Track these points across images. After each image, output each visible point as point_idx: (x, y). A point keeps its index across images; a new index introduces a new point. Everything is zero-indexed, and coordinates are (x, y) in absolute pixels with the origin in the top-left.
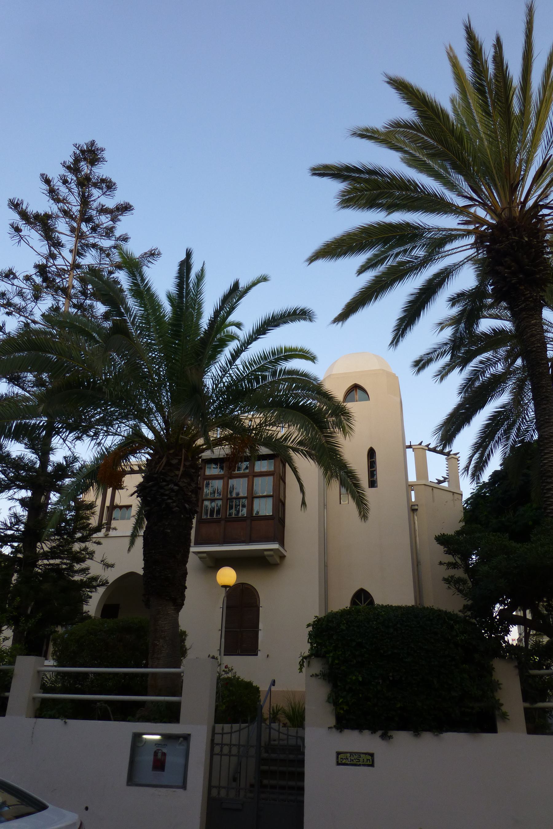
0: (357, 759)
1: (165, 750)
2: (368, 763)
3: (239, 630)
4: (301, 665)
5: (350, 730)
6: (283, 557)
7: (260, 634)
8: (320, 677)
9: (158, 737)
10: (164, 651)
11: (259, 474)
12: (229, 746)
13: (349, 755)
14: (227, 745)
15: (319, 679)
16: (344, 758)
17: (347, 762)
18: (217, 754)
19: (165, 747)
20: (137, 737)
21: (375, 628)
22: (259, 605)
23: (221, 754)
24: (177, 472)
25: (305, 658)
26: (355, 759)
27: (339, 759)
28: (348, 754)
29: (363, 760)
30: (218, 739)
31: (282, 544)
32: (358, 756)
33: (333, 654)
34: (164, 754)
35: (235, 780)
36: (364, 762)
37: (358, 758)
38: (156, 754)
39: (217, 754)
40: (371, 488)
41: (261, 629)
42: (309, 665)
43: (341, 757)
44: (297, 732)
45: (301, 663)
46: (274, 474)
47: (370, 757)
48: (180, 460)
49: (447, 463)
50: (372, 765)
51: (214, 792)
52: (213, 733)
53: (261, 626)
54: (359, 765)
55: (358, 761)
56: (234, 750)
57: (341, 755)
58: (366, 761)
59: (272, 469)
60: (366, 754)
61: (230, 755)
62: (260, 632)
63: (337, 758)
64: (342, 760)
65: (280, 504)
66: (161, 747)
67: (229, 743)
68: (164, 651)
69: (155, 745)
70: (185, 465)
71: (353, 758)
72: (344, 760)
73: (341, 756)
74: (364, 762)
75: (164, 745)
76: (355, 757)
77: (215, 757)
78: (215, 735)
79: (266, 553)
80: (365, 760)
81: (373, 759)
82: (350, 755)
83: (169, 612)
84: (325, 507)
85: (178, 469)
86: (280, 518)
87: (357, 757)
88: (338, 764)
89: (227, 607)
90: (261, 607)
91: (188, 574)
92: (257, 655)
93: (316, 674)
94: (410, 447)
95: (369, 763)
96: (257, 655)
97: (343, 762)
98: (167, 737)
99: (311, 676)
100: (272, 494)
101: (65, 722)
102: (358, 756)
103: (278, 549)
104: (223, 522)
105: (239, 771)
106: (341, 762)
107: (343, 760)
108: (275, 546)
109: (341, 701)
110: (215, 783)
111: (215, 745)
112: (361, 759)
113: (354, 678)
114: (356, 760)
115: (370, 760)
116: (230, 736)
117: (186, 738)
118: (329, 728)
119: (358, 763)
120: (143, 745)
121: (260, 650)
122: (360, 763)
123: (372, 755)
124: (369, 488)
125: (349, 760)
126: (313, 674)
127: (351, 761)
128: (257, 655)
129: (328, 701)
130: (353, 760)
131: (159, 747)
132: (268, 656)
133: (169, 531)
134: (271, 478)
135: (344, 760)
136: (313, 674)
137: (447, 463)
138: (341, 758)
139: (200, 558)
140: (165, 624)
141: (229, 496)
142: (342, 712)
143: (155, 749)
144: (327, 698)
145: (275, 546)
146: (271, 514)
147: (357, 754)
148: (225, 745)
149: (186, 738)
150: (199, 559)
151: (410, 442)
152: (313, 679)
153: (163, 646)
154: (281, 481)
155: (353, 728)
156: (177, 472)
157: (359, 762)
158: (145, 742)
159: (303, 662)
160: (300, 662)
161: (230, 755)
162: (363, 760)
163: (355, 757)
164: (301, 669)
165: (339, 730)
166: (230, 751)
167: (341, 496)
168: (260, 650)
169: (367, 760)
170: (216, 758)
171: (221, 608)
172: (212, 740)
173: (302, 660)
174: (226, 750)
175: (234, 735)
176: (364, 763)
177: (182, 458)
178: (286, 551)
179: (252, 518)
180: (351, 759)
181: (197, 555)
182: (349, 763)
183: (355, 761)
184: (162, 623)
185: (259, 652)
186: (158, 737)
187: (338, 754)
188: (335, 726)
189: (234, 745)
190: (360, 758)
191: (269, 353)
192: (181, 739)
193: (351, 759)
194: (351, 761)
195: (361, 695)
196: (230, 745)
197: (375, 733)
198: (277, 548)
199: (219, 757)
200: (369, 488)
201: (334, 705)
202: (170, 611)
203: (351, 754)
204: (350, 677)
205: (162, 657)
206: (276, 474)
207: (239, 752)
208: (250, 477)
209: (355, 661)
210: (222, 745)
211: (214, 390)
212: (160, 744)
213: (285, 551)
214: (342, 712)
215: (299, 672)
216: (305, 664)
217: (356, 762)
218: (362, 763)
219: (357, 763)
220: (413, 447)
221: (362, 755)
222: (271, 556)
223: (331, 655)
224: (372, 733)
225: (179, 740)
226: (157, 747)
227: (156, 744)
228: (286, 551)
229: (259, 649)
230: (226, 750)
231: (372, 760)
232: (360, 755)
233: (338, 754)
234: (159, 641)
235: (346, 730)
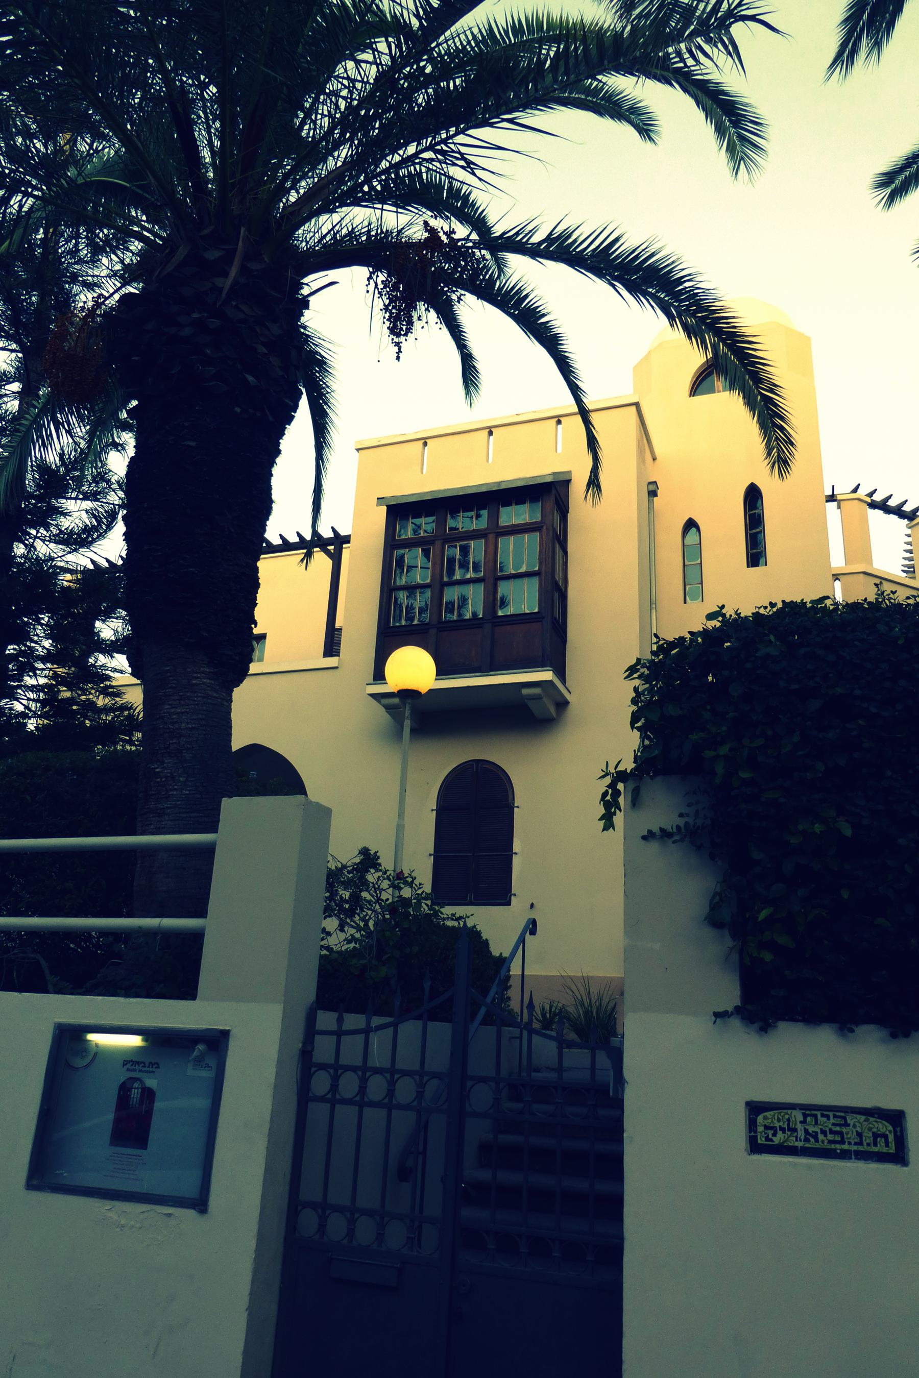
0: (832, 1132)
1: (151, 1082)
2: (881, 1147)
4: (610, 805)
5: (800, 1025)
6: (562, 705)
7: (516, 861)
8: (677, 838)
9: (135, 1041)
10: (176, 790)
11: (510, 529)
12: (360, 1073)
13: (798, 1115)
14: (354, 1069)
15: (674, 842)
16: (777, 1125)
17: (792, 1142)
18: (322, 1099)
19: (153, 1072)
21: (901, 642)
22: (514, 804)
23: (333, 1099)
24: (219, 281)
25: (621, 776)
26: (824, 1132)
27: (760, 1129)
28: (794, 1113)
29: (859, 1135)
30: (324, 1049)
31: (561, 673)
32: (839, 1121)
33: (731, 750)
34: (149, 1095)
35: (404, 1174)
36: (861, 1143)
37: (838, 1129)
38: (124, 1089)
39: (322, 1099)
40: (752, 567)
41: (517, 851)
42: (635, 802)
43: (767, 1122)
45: (608, 798)
46: (542, 527)
47: (884, 1127)
48: (232, 254)
49: (909, 531)
50: (899, 1157)
51: (309, 1221)
52: (311, 1032)
53: (517, 846)
54: (844, 1155)
55: (838, 1138)
56: (405, 1090)
57: (768, 1114)
58: (871, 1140)
59: (538, 517)
60: (868, 1112)
61: (389, 1104)
62: (515, 858)
63: (752, 1125)
64: (770, 1132)
65: (556, 595)
66: (140, 1071)
67: (358, 1062)
68: (176, 790)
69: (124, 1065)
70: (243, 269)
71: (817, 1129)
72: (780, 1133)
73: (765, 1118)
74: (861, 1143)
76: (828, 1124)
77: (312, 1106)
78: (317, 1037)
79: (525, 691)
80: (868, 1137)
81: (902, 1131)
82: (805, 1116)
83: (194, 682)
84: (654, 606)
85: (225, 274)
86: (555, 618)
87: (834, 1124)
88: (755, 1147)
89: (380, 680)
90: (518, 807)
91: (261, 586)
92: (510, 904)
93: (662, 830)
94: (831, 498)
95: (885, 1150)
97: (776, 1140)
99: (644, 838)
100: (537, 569)
102: (839, 1121)
103: (551, 682)
104: (433, 632)
105: (421, 1149)
106: (767, 1139)
107: (775, 1135)
108: (547, 675)
109: (763, 915)
110: (311, 1191)
111: (313, 1069)
112: (850, 1134)
113: (818, 828)
114: (830, 1137)
115: (885, 1137)
116: (329, 1029)
118: (717, 1015)
119: (838, 1146)
120: (86, 1066)
121: (515, 895)
122: (846, 1147)
123: (896, 1118)
124: (748, 567)
125: (801, 1134)
126: (650, 832)
127: (807, 1140)
129: (714, 920)
130: (815, 1136)
131: (135, 1070)
132: (532, 906)
133: (193, 444)
134: (536, 536)
135: (780, 1133)
136: (650, 832)
137: (909, 531)
138: (766, 1127)
139: (388, 708)
140: (182, 713)
141: (445, 579)
142: (768, 957)
143: (123, 1076)
144: (707, 909)
145: (547, 675)
146: (536, 610)
147: (831, 1114)
148: (347, 1068)
150: (384, 709)
151: (833, 486)
152: (653, 847)
153: (173, 778)
154: (557, 546)
156: (219, 281)
157: (842, 1142)
158: (96, 1054)
159: (616, 793)
160: (605, 794)
161: (389, 1104)
162: (859, 1135)
163: (828, 1124)
164: (608, 821)
165: (756, 1026)
166: (391, 1093)
167: (687, 587)
168: (515, 895)
169: (876, 1136)
170: (319, 1112)
171: (432, 810)
172: (306, 1054)
173: (612, 786)
174: (349, 1085)
175: (375, 1040)
176: (861, 1148)
177: (235, 250)
178: (570, 693)
179: (494, 621)
180: (806, 1131)
181: (380, 702)
182: (799, 1144)
183: (823, 1142)
184: (173, 710)
185: (513, 898)
186: (135, 1041)
187: (755, 1109)
188: (738, 1010)
189: (406, 1073)
190: (844, 1130)
191: (506, 32)
192: (201, 1047)
193: (806, 1131)
194: (807, 1140)
195: (845, 894)
196: (392, 1073)
197: (907, 1035)
198: (551, 679)
199: (326, 1107)
200: (748, 567)
201: (734, 936)
202: (198, 678)
203: (808, 1110)
204: (801, 827)
205: (167, 808)
206: (545, 528)
207: (420, 1095)
208: (491, 537)
209: (820, 766)
210: (336, 1069)
211: (378, 235)
212: (138, 1063)
213: (568, 693)
214: (768, 957)
215: (603, 831)
216: (621, 800)
217: (830, 1142)
218: (855, 1148)
219: (833, 1146)
220: (839, 497)
222: (537, 698)
223: (724, 750)
224: (894, 1036)
225: (194, 1051)
226: (128, 1070)
227: (125, 1063)
228: (570, 693)
230: (349, 1085)
231: (896, 1137)
232: (845, 1118)
233: (755, 1109)
234: (163, 763)
235: (782, 1025)
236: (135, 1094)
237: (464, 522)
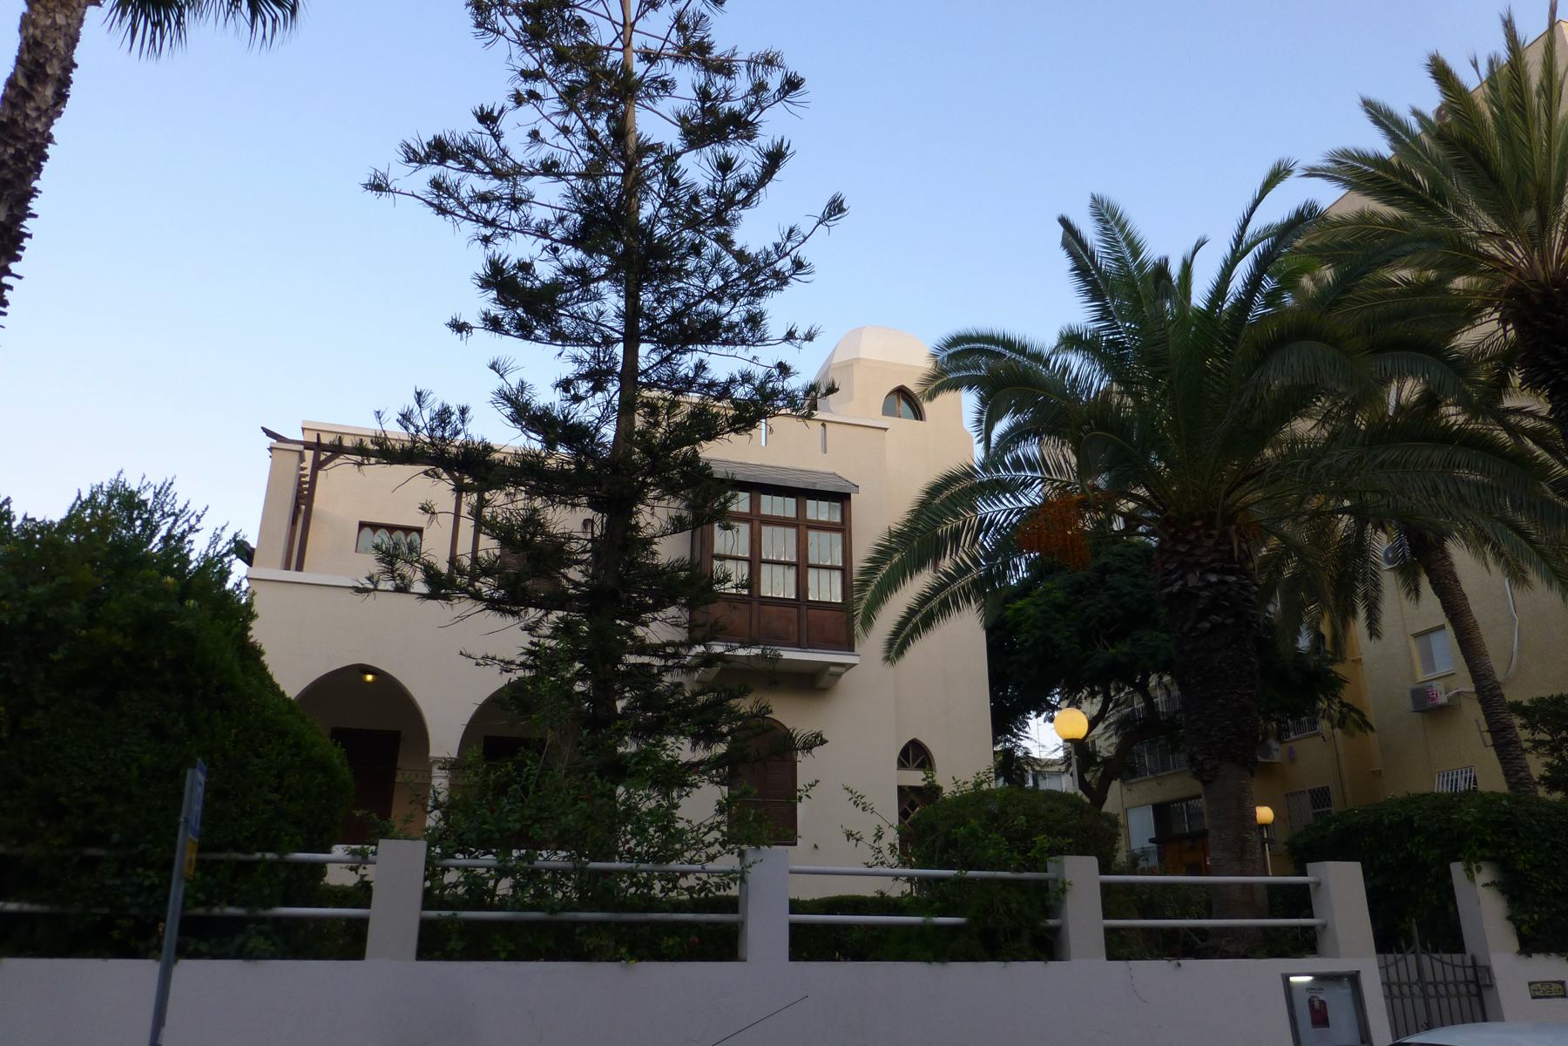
1: (1322, 997)
3: (761, 800)
9: (1308, 979)
13: (1539, 985)
20: (1286, 978)
34: (1323, 1003)
38: (1311, 1002)
44: (1463, 962)
47: (1561, 987)
75: (1319, 989)
88: (1534, 997)
96: (796, 844)
98: (1321, 978)
101: (1179, 965)
117: (1354, 979)
121: (800, 837)
123: (1562, 983)
128: (796, 844)
143: (1308, 996)
149: (1354, 979)
152: (1485, 889)
155: (1538, 951)
163: (1547, 987)
168: (800, 837)
186: (1308, 979)
187: (1530, 984)
212: (1313, 989)
221: (1553, 985)
227: (1307, 989)
229: (798, 834)
233: (1530, 984)
236: (1317, 1004)
237: (771, 505)
